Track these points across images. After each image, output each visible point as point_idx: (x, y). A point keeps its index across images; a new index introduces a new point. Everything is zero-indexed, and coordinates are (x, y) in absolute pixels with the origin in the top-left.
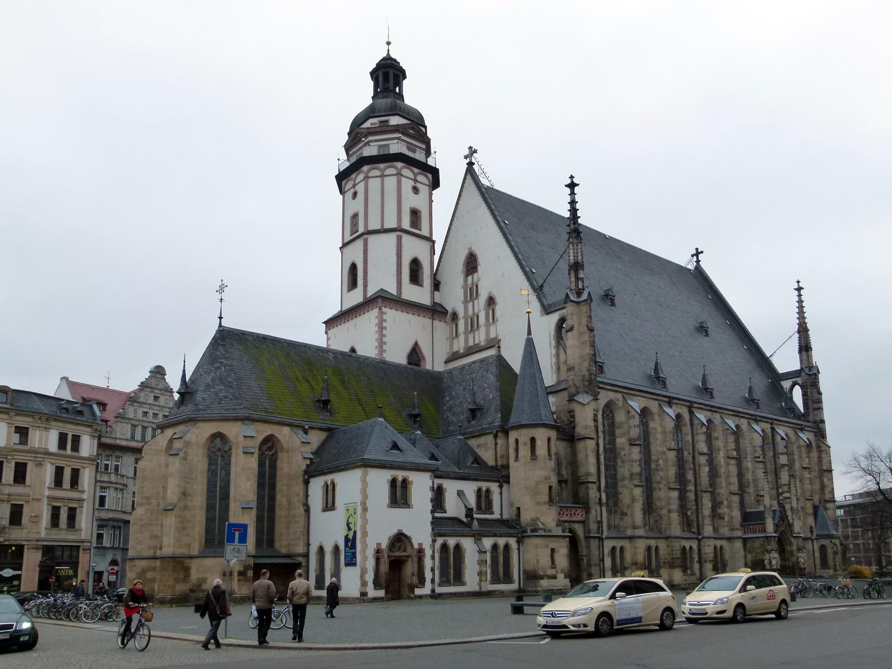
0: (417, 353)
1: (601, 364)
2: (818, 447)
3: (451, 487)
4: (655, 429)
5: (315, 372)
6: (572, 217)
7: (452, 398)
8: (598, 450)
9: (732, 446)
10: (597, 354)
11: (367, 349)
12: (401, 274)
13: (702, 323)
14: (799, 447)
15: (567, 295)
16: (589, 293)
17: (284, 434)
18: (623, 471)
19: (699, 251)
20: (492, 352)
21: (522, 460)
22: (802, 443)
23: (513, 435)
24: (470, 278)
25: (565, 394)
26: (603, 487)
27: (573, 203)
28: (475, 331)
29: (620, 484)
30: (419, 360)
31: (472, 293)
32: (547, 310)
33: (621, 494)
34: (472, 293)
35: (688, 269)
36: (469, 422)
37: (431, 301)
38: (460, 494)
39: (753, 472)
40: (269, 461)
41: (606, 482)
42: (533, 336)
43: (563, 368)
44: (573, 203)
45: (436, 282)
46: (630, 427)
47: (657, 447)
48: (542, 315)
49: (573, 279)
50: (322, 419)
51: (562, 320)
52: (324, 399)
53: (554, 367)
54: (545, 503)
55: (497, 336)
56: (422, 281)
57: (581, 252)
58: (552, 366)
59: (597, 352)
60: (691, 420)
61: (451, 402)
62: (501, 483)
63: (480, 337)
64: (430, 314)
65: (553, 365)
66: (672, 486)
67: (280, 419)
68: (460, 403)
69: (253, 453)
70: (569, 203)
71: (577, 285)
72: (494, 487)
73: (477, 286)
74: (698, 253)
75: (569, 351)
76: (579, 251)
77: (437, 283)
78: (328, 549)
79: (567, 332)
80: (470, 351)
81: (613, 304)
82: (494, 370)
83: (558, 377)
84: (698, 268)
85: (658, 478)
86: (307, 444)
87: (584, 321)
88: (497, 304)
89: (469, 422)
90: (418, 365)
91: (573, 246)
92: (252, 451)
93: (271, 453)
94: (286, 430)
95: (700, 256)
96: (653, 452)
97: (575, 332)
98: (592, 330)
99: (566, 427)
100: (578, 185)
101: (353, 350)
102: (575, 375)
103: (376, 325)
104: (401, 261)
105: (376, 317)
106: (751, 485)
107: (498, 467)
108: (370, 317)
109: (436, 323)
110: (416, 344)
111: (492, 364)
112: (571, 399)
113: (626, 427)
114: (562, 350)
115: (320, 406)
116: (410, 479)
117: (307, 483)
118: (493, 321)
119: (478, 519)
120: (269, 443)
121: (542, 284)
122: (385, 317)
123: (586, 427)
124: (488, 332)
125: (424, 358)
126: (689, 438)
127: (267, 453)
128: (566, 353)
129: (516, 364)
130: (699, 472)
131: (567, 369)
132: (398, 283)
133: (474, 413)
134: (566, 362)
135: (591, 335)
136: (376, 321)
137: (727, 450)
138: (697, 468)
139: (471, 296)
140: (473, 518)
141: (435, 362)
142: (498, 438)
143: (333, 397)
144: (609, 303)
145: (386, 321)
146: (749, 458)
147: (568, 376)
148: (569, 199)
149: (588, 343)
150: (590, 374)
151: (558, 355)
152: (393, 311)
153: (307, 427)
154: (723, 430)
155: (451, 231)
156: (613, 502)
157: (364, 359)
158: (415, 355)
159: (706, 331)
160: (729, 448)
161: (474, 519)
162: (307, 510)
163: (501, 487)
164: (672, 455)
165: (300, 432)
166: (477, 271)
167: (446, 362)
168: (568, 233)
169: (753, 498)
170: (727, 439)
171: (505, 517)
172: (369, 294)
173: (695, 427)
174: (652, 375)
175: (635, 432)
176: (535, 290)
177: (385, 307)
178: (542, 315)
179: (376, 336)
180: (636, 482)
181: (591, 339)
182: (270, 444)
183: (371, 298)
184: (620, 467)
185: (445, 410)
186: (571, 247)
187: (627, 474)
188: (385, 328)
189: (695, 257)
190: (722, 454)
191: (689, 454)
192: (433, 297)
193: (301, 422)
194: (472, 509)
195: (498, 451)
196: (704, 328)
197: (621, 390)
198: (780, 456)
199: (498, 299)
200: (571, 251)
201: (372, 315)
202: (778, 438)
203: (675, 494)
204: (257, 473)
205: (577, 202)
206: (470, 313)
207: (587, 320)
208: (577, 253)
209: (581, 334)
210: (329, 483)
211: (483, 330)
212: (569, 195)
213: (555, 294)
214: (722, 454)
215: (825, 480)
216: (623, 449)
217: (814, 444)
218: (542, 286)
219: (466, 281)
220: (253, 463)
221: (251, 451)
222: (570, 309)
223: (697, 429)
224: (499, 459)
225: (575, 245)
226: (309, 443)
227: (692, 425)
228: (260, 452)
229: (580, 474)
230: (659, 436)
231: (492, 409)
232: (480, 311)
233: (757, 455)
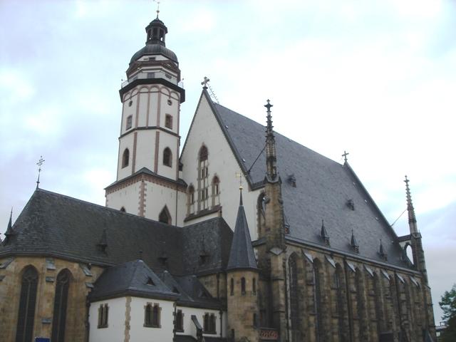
3: (188, 313)
4: (323, 274)
8: (286, 288)
9: (371, 287)
11: (133, 210)
14: (412, 288)
18: (303, 304)
20: (215, 216)
21: (236, 295)
22: (414, 286)
24: (202, 163)
25: (264, 248)
26: (289, 316)
27: (269, 117)
30: (167, 219)
31: (203, 173)
32: (253, 187)
34: (203, 173)
38: (194, 318)
39: (385, 306)
42: (243, 205)
43: (263, 228)
44: (269, 117)
46: (306, 272)
47: (324, 287)
48: (249, 191)
49: (269, 167)
51: (262, 195)
54: (251, 326)
60: (345, 268)
63: (208, 204)
66: (335, 315)
71: (272, 172)
72: (217, 313)
73: (207, 169)
75: (267, 217)
81: (294, 186)
83: (259, 236)
85: (326, 309)
96: (322, 290)
97: (271, 204)
98: (281, 203)
101: (123, 209)
106: (384, 315)
113: (304, 271)
116: (160, 306)
117: (88, 306)
123: (278, 271)
124: (213, 202)
125: (170, 218)
128: (265, 219)
129: (232, 225)
133: (204, 258)
134: (264, 224)
141: (178, 221)
146: (382, 296)
150: (281, 234)
151: (259, 219)
152: (151, 183)
156: (297, 325)
158: (165, 214)
163: (221, 314)
164: (333, 293)
169: (385, 324)
170: (367, 282)
171: (224, 336)
172: (137, 170)
176: (245, 174)
178: (249, 191)
179: (139, 200)
180: (311, 312)
187: (305, 306)
188: (146, 195)
190: (365, 293)
192: (178, 175)
195: (220, 286)
199: (220, 179)
203: (336, 321)
206: (202, 187)
209: (275, 205)
211: (210, 200)
213: (258, 177)
214: (365, 293)
215: (429, 311)
217: (421, 287)
222: (267, 188)
226: (91, 276)
227: (346, 272)
230: (325, 279)
232: (208, 186)
233: (387, 293)
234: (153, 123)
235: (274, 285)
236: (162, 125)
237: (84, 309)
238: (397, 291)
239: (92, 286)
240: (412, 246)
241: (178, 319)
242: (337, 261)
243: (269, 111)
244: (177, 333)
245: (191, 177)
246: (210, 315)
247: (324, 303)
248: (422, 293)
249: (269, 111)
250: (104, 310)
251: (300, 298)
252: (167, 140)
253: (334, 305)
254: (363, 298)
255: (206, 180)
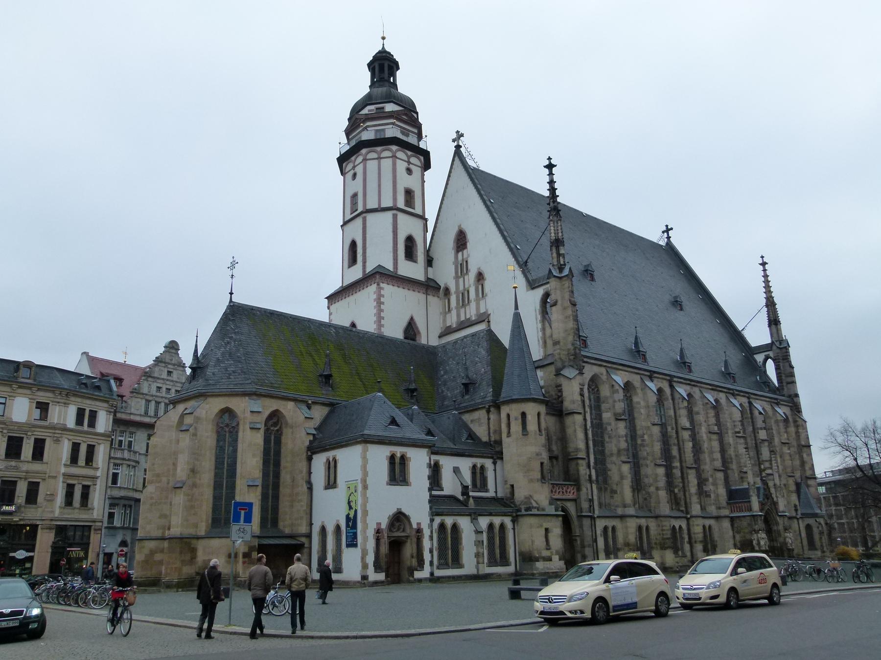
0: (413, 329)
1: (584, 339)
2: (795, 421)
3: (447, 463)
4: (639, 403)
5: (318, 347)
6: (551, 196)
7: (446, 372)
8: (586, 425)
9: (713, 420)
10: (580, 328)
11: (367, 325)
12: (397, 250)
13: (676, 297)
14: (777, 422)
15: (550, 270)
16: (570, 268)
17: (288, 409)
18: (611, 447)
19: (669, 227)
20: (482, 327)
22: (779, 418)
23: (505, 410)
25: (552, 369)
26: (592, 464)
27: (552, 182)
28: (466, 305)
29: (608, 460)
30: (415, 335)
31: (462, 269)
32: (532, 285)
33: (610, 470)
34: (462, 269)
35: (660, 245)
36: (463, 396)
37: (425, 276)
38: (456, 470)
40: (275, 437)
41: (595, 458)
42: (520, 310)
43: (549, 342)
44: (552, 182)
45: (429, 258)
48: (527, 291)
49: (555, 255)
50: (324, 394)
51: (547, 295)
52: (326, 373)
53: (541, 341)
55: (487, 310)
57: (561, 229)
58: (539, 341)
59: (580, 325)
60: (672, 395)
61: (445, 376)
62: (494, 460)
64: (424, 289)
65: (540, 339)
67: (285, 394)
68: (454, 377)
69: (260, 429)
70: (548, 183)
71: (559, 261)
72: (488, 463)
73: (467, 262)
74: (668, 230)
75: (553, 325)
76: (559, 228)
77: (431, 259)
78: (330, 529)
79: (551, 306)
80: (462, 326)
81: (592, 279)
82: (485, 344)
83: (545, 352)
84: (669, 245)
86: (310, 420)
87: (567, 296)
88: (485, 280)
89: (463, 396)
90: (414, 340)
91: (554, 224)
92: (258, 426)
93: (276, 429)
94: (291, 405)
95: (670, 232)
96: (638, 428)
97: (559, 306)
98: (574, 305)
99: (554, 401)
100: (555, 166)
101: (353, 325)
102: (560, 349)
103: (375, 300)
104: (397, 238)
105: (375, 293)
107: (492, 443)
108: (369, 293)
109: (430, 298)
110: (412, 319)
111: (482, 338)
112: (558, 374)
114: (547, 324)
115: (322, 380)
117: (310, 459)
118: (483, 296)
119: (474, 497)
120: (275, 417)
121: (527, 260)
122: (382, 292)
124: (478, 308)
125: (419, 333)
126: (672, 412)
127: (272, 428)
128: (551, 327)
129: (505, 338)
130: (684, 448)
131: (553, 343)
132: (394, 259)
133: (468, 387)
134: (551, 336)
135: (573, 310)
136: (375, 296)
137: (709, 425)
138: (681, 443)
139: (461, 272)
140: (469, 497)
141: (429, 337)
142: (490, 413)
143: (335, 375)
144: (589, 278)
145: (383, 296)
146: (730, 432)
147: (555, 350)
148: (547, 179)
149: (571, 318)
150: (575, 349)
151: (543, 329)
152: (391, 287)
153: (310, 402)
154: (703, 405)
157: (364, 334)
158: (411, 330)
159: (681, 305)
160: (710, 423)
161: (469, 497)
162: (310, 488)
163: (495, 463)
164: (656, 430)
165: (304, 407)
167: (440, 337)
168: (548, 211)
172: (368, 270)
173: (676, 402)
174: (632, 349)
175: (620, 407)
176: (520, 266)
177: (383, 283)
178: (527, 291)
179: (375, 311)
180: (624, 458)
181: (574, 314)
182: (275, 420)
183: (370, 274)
184: (607, 442)
185: (440, 385)
186: (552, 225)
187: (615, 450)
188: (383, 303)
189: (666, 234)
191: (672, 429)
193: (304, 397)
194: (468, 487)
195: (491, 426)
196: (679, 303)
197: (604, 364)
198: (760, 431)
199: (486, 276)
200: (552, 228)
201: (371, 290)
202: (756, 413)
204: (262, 449)
205: (555, 182)
206: (461, 288)
207: (570, 295)
208: (558, 230)
209: (565, 308)
210: (331, 460)
211: (473, 305)
212: (548, 175)
213: (539, 270)
216: (610, 424)
217: (790, 419)
218: (526, 262)
220: (258, 438)
221: (258, 427)
222: (553, 284)
223: (678, 403)
224: (492, 435)
225: (556, 222)
226: (312, 418)
227: (673, 399)
228: (266, 428)
229: (570, 450)
230: (643, 411)
231: (484, 383)
232: (470, 286)
233: (737, 430)
234: (387, 202)
235: (569, 421)
236: (401, 204)
237: (304, 464)
238: (753, 426)
239: (314, 432)
240: (774, 360)
241: (435, 472)
242: (660, 385)
243: (551, 174)
244: (434, 493)
245: (445, 273)
246: (479, 466)
247: (642, 445)
248: (792, 429)
249: (551, 174)
250: (332, 464)
251: (607, 439)
252: (408, 226)
253: (657, 447)
254: (702, 437)
255: (466, 277)
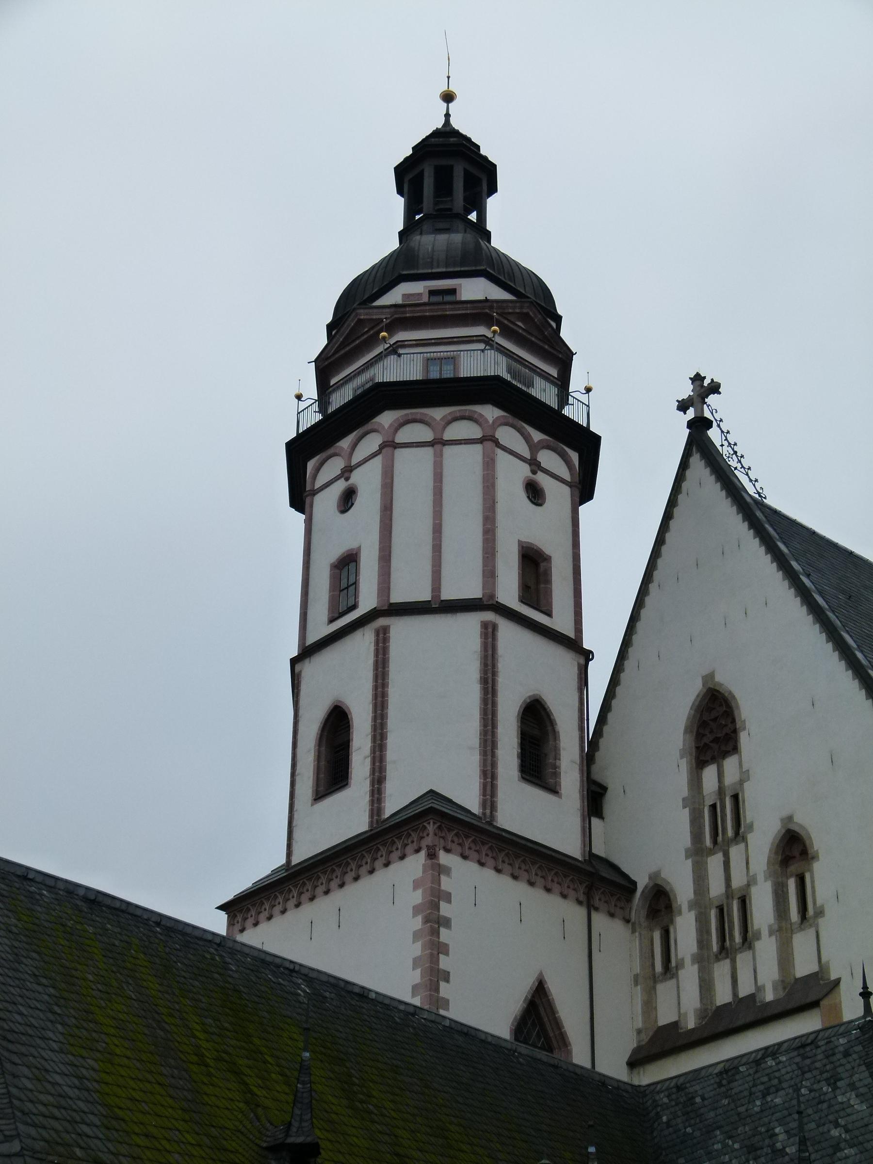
24: (710, 774)
56: (556, 775)
73: (736, 798)
155: (640, 626)
166: (735, 749)
199: (819, 842)
219: (696, 782)
